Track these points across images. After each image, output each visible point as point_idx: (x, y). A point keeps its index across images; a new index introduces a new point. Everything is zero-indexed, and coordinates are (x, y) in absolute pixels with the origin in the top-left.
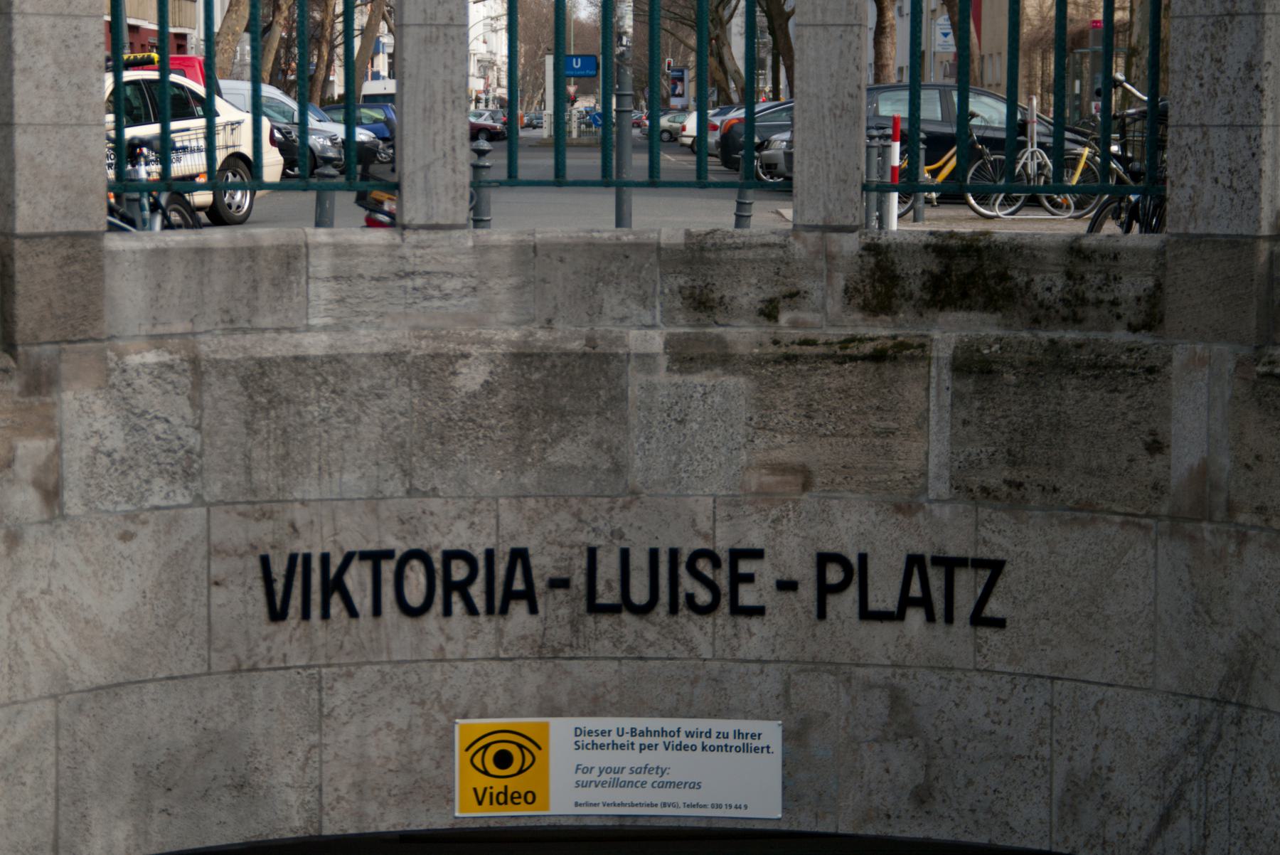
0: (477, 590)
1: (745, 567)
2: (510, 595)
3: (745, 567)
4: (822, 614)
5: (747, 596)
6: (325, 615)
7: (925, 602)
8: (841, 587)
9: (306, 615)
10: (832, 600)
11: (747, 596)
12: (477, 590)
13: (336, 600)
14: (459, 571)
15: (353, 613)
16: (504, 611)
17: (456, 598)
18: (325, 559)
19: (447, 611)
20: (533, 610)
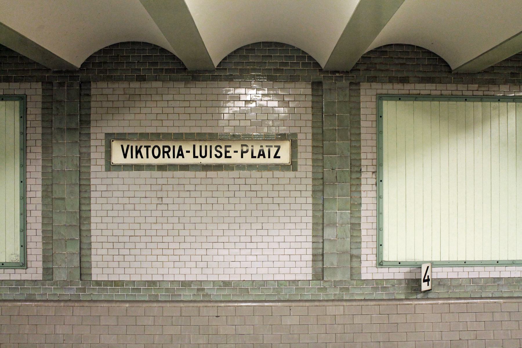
0: (171, 153)
1: (228, 149)
2: (179, 155)
3: (228, 149)
4: (242, 157)
5: (228, 155)
6: (137, 157)
7: (264, 155)
8: (247, 152)
9: (132, 157)
11: (228, 155)
12: (171, 153)
13: (139, 155)
14: (166, 149)
15: (142, 157)
16: (177, 157)
17: (166, 154)
19: (164, 157)
20: (183, 157)
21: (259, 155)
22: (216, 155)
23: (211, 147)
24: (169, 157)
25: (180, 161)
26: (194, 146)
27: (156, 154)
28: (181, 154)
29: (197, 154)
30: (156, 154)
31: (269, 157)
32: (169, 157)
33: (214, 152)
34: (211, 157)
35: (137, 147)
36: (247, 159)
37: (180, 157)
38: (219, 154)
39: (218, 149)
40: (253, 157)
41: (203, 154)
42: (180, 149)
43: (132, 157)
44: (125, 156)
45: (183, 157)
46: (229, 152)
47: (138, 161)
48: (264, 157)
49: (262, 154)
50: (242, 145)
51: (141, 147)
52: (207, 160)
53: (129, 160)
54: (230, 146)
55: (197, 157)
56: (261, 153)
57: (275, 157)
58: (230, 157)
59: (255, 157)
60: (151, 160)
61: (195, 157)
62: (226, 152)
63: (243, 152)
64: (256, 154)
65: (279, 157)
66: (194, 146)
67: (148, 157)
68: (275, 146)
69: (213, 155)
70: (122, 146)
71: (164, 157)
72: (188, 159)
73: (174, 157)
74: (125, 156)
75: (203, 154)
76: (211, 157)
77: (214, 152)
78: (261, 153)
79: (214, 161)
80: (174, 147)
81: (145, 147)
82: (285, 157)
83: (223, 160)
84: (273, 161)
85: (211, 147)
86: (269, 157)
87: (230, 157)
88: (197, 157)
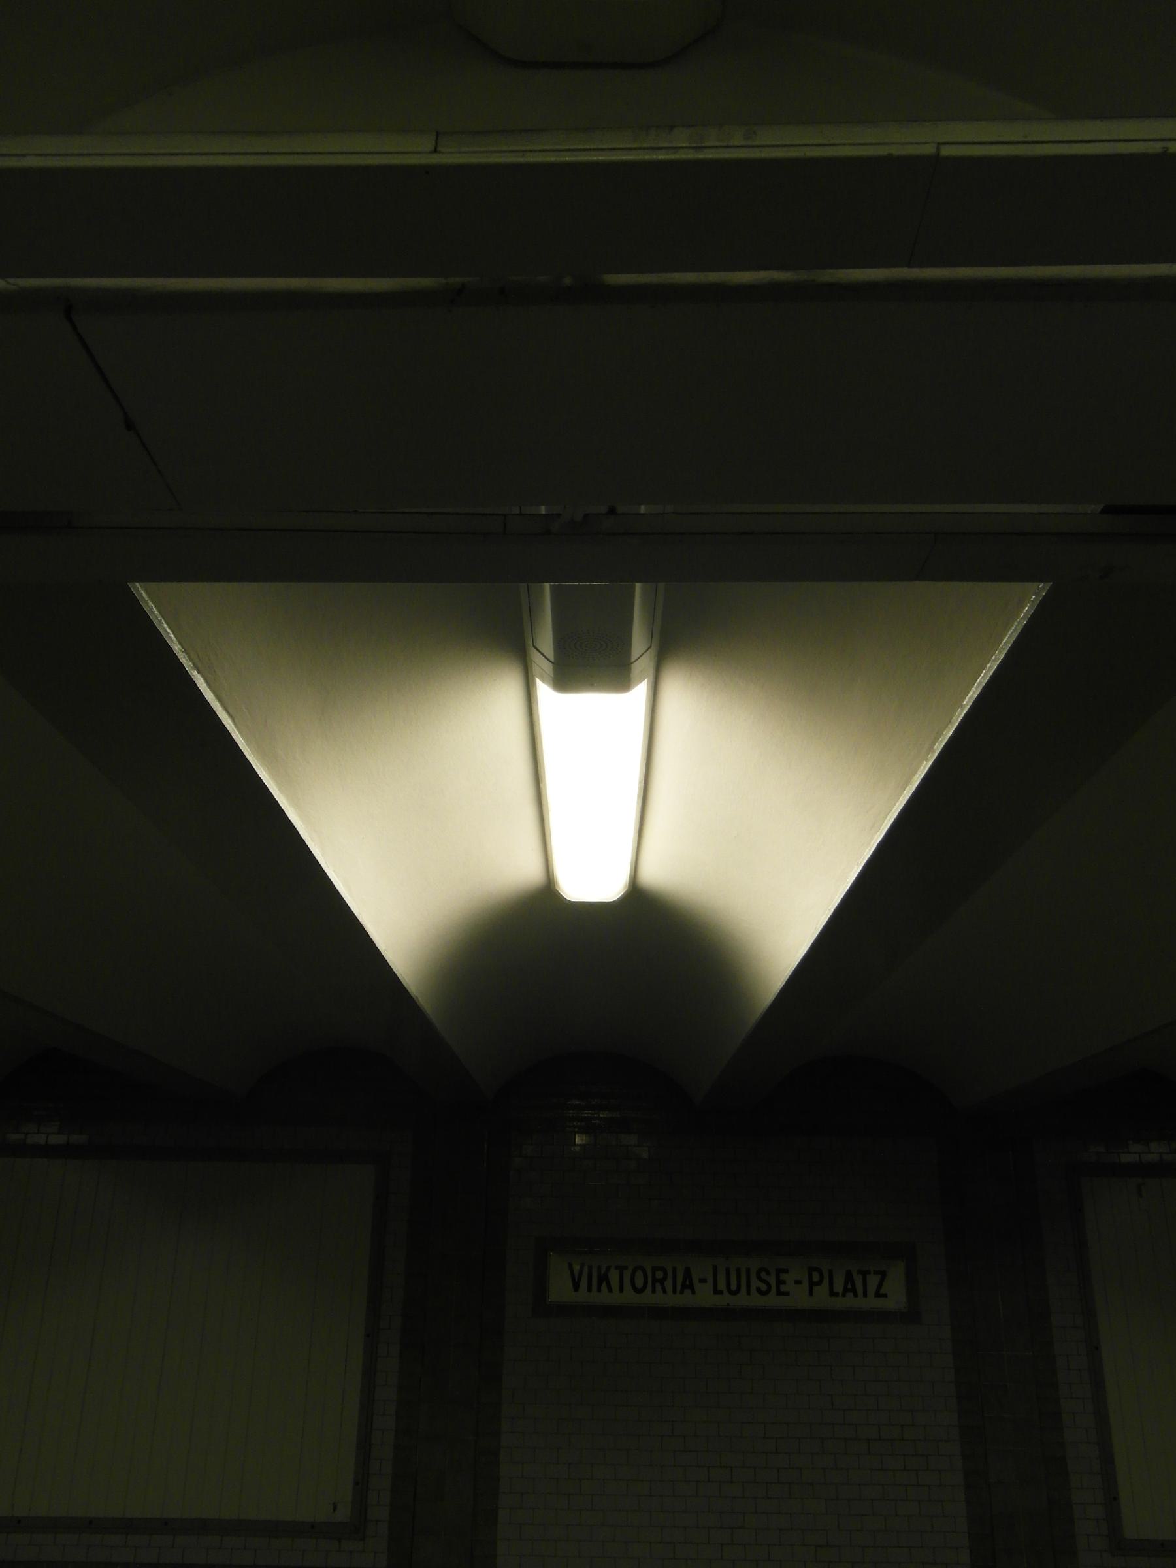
0: (669, 1284)
1: (784, 1277)
2: (684, 1287)
3: (784, 1277)
4: (811, 1293)
5: (783, 1288)
6: (599, 1290)
8: (819, 1283)
9: (590, 1289)
10: (815, 1288)
11: (783, 1288)
12: (669, 1284)
14: (659, 1275)
15: (610, 1290)
16: (682, 1292)
17: (658, 1286)
18: (599, 1268)
19: (654, 1291)
20: (693, 1292)
21: (846, 1290)
22: (758, 1290)
23: (748, 1271)
24: (665, 1292)
25: (685, 1299)
26: (715, 1269)
27: (639, 1283)
28: (688, 1285)
29: (722, 1285)
30: (639, 1283)
31: (865, 1295)
32: (665, 1292)
33: (755, 1283)
34: (749, 1293)
35: (599, 1268)
36: (821, 1298)
37: (688, 1292)
38: (764, 1287)
39: (763, 1275)
40: (833, 1294)
41: (734, 1287)
42: (688, 1274)
43: (590, 1289)
44: (576, 1287)
45: (693, 1292)
46: (784, 1282)
47: (604, 1297)
48: (856, 1295)
49: (850, 1288)
50: (811, 1270)
51: (608, 1269)
52: (742, 1300)
53: (582, 1296)
54: (786, 1271)
55: (721, 1293)
56: (849, 1286)
57: (878, 1295)
58: (787, 1294)
59: (837, 1294)
60: (628, 1297)
61: (717, 1292)
62: (780, 1282)
63: (812, 1284)
64: (839, 1287)
65: (885, 1296)
66: (715, 1269)
67: (621, 1290)
68: (876, 1273)
69: (753, 1289)
70: (570, 1266)
71: (654, 1291)
72: (704, 1297)
73: (674, 1291)
74: (576, 1287)
75: (734, 1287)
76: (749, 1293)
77: (755, 1283)
78: (849, 1286)
79: (757, 1301)
80: (674, 1270)
81: (617, 1268)
82: (895, 1297)
83: (773, 1301)
84: (872, 1303)
85: (748, 1271)
86: (865, 1295)
87: (787, 1294)
88: (721, 1293)
